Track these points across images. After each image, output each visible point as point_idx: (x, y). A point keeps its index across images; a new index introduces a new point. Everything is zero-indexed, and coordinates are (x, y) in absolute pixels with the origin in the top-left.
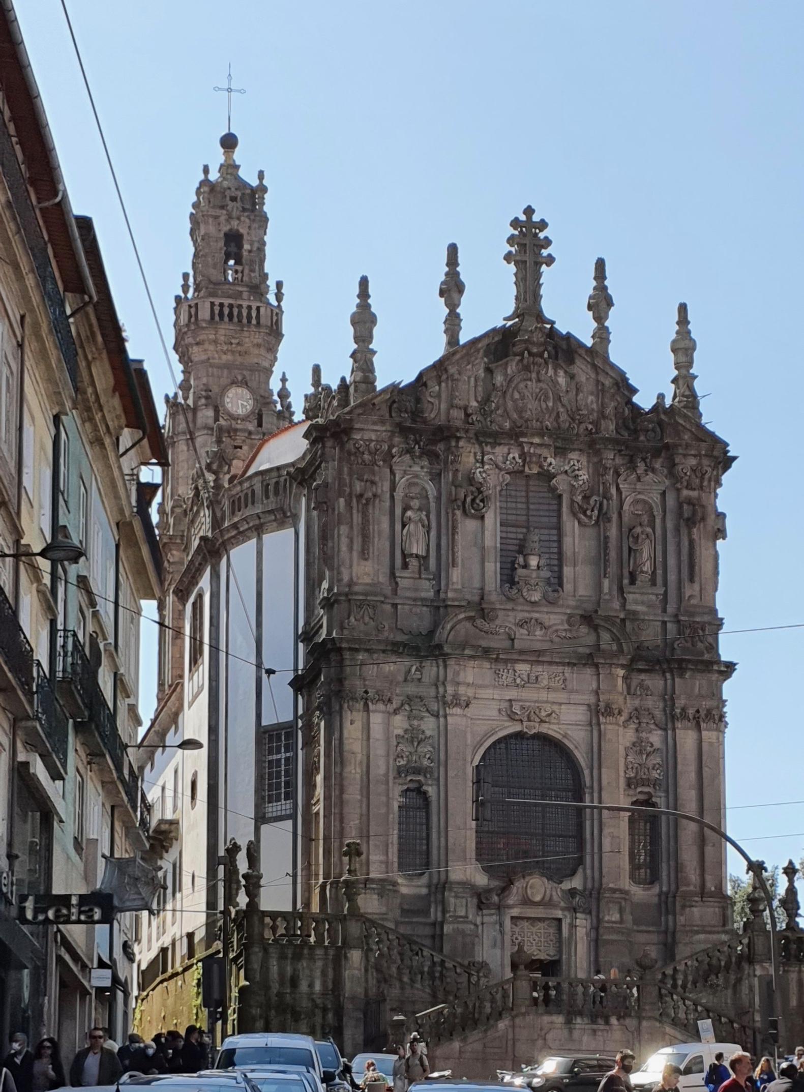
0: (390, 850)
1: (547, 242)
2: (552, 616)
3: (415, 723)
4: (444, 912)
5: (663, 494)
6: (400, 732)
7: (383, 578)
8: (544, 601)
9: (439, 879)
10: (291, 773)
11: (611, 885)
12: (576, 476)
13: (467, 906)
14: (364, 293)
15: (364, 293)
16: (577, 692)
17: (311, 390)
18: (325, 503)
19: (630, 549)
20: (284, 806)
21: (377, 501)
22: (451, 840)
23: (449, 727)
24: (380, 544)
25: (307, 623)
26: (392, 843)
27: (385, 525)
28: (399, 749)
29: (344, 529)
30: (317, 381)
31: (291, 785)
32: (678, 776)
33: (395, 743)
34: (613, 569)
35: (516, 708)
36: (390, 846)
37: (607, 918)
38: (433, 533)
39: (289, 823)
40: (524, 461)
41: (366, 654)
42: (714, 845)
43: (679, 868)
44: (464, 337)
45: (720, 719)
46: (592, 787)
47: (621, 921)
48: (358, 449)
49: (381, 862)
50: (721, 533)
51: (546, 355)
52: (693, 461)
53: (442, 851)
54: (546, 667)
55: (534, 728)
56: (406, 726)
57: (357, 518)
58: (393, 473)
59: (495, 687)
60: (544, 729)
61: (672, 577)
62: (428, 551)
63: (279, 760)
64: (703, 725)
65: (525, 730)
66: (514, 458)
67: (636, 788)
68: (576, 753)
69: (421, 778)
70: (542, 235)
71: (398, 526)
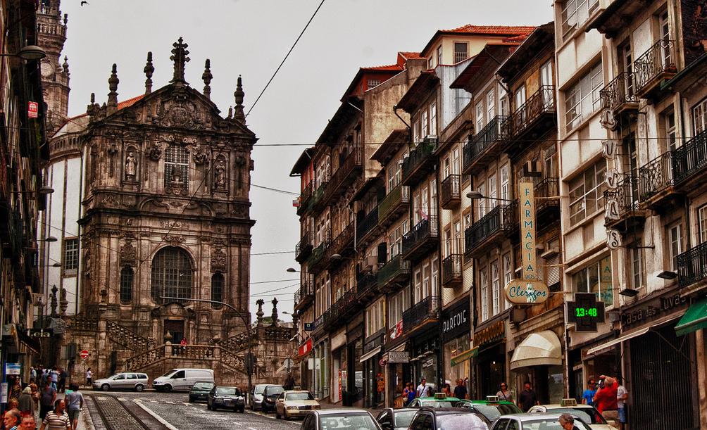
1: (188, 53)
4: (138, 317)
5: (229, 153)
6: (122, 245)
8: (181, 195)
10: (76, 258)
12: (195, 146)
14: (114, 70)
15: (114, 70)
16: (193, 231)
17: (90, 103)
20: (73, 271)
24: (117, 170)
25: (85, 198)
27: (119, 163)
29: (103, 164)
30: (93, 100)
31: (76, 262)
34: (209, 182)
35: (169, 236)
38: (138, 167)
39: (75, 278)
40: (175, 139)
43: (231, 301)
44: (153, 89)
45: (248, 244)
47: (208, 322)
50: (252, 168)
56: (125, 243)
57: (108, 160)
59: (160, 229)
61: (232, 185)
62: (135, 173)
63: (71, 252)
70: (185, 50)
71: (124, 164)
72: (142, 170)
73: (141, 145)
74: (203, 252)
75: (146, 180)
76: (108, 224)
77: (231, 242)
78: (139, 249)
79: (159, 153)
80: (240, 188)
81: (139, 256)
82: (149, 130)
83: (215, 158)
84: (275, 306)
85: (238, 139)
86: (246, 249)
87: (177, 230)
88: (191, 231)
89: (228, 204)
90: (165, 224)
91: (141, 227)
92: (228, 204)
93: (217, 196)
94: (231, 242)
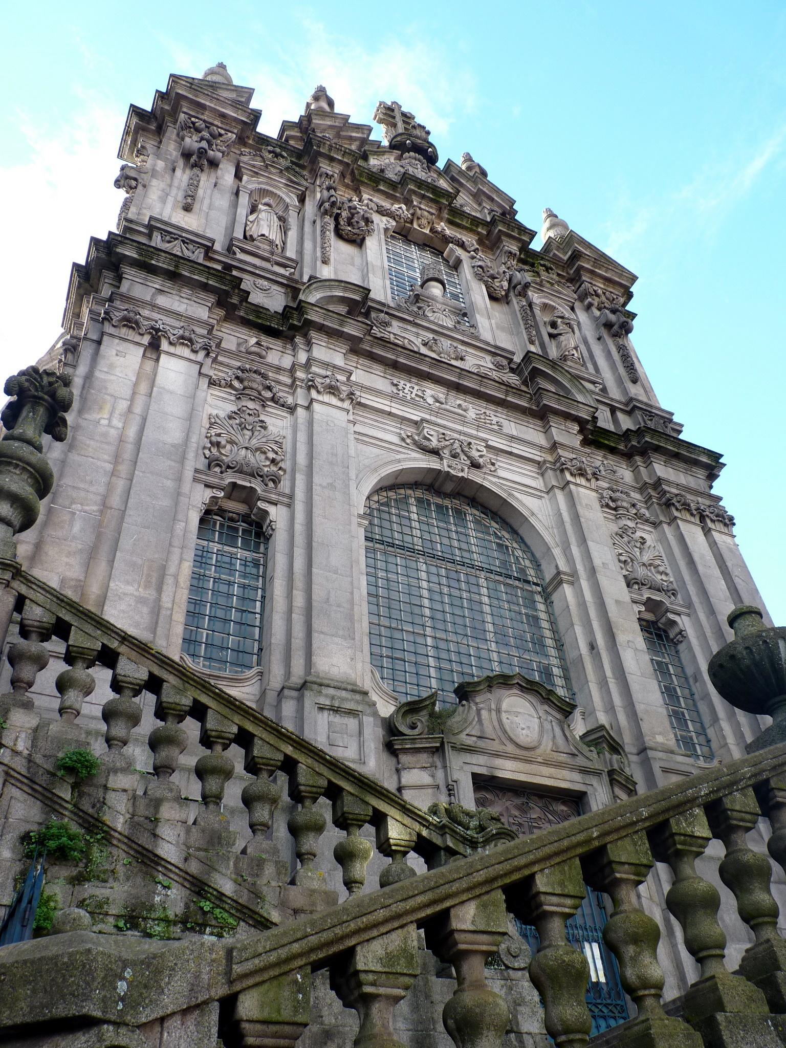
0: (168, 589)
2: (469, 350)
3: (251, 405)
5: (572, 309)
9: (288, 674)
11: (660, 739)
13: (360, 733)
18: (136, 179)
19: (551, 336)
21: (213, 175)
22: (318, 593)
23: (316, 416)
26: (176, 577)
28: (213, 432)
32: (704, 580)
33: (208, 426)
36: (169, 580)
38: (292, 235)
40: (413, 215)
41: (168, 284)
46: (574, 574)
48: (193, 123)
49: (141, 600)
51: (430, 150)
52: (602, 286)
53: (298, 619)
54: (469, 398)
55: (460, 470)
60: (476, 477)
65: (447, 469)
66: (400, 208)
68: (532, 520)
69: (257, 485)
72: (308, 245)
73: (302, 200)
74: (581, 511)
76: (154, 307)
77: (668, 504)
78: (302, 437)
81: (302, 459)
82: (332, 159)
88: (512, 438)
89: (613, 410)
90: (409, 387)
91: (307, 366)
94: (668, 504)
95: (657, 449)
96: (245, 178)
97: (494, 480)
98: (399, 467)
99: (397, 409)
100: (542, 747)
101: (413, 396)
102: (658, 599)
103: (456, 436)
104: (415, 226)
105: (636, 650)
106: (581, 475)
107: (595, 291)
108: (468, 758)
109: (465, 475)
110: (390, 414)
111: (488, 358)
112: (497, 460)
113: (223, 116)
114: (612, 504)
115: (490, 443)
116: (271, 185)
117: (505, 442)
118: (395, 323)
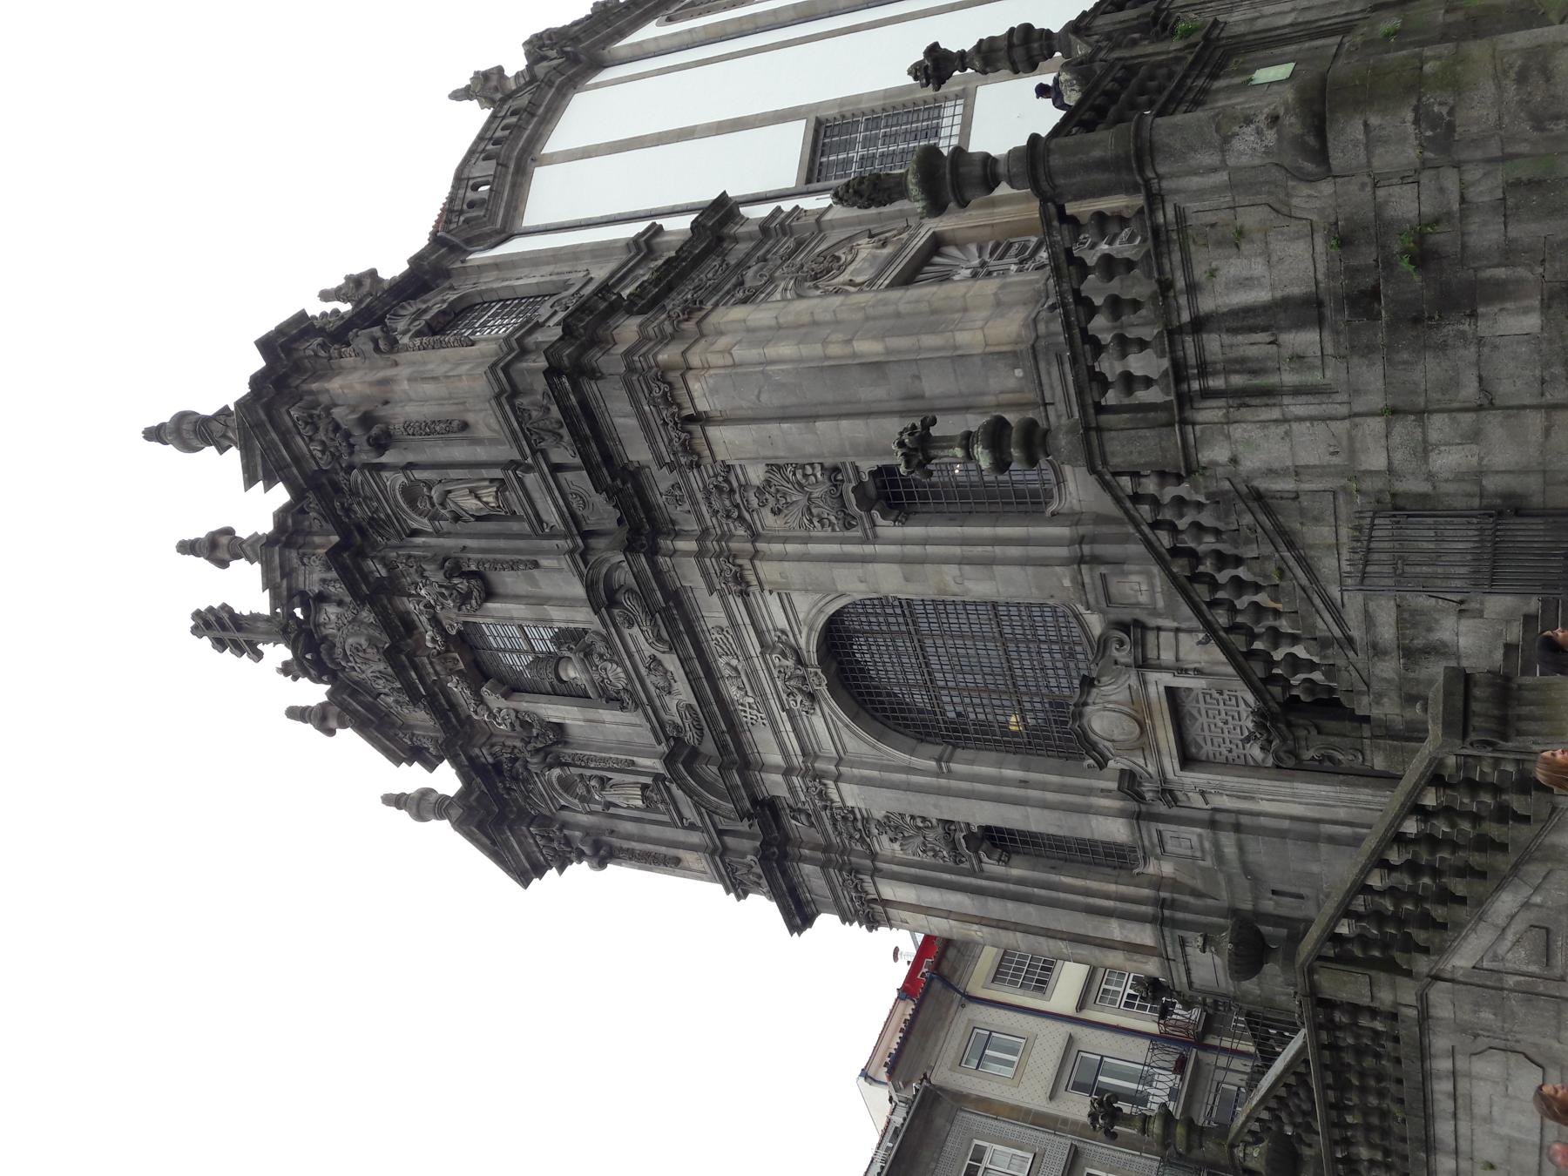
2: (633, 649)
6: (896, 846)
7: (695, 838)
11: (1067, 583)
21: (605, 838)
36: (1091, 900)
37: (1143, 599)
38: (609, 775)
42: (918, 377)
49: (1122, 927)
56: (885, 839)
58: (563, 808)
59: (776, 733)
60: (812, 657)
64: (689, 411)
67: (854, 518)
68: (832, 609)
75: (633, 763)
79: (525, 725)
80: (465, 426)
83: (423, 523)
84: (962, 60)
85: (297, 460)
86: (696, 387)
87: (752, 673)
90: (746, 716)
92: (556, 468)
93: (551, 516)
95: (608, 459)
96: (563, 803)
97: (802, 642)
98: (852, 725)
99: (786, 726)
100: (1133, 713)
101: (755, 712)
102: (852, 496)
103: (779, 683)
104: (461, 666)
105: (962, 575)
106: (742, 576)
107: (323, 452)
108: (1170, 776)
109: (819, 671)
110: (794, 730)
111: (626, 632)
112: (769, 631)
113: (520, 843)
114: (735, 514)
115: (758, 650)
116: (554, 789)
117: (744, 632)
118: (666, 717)
